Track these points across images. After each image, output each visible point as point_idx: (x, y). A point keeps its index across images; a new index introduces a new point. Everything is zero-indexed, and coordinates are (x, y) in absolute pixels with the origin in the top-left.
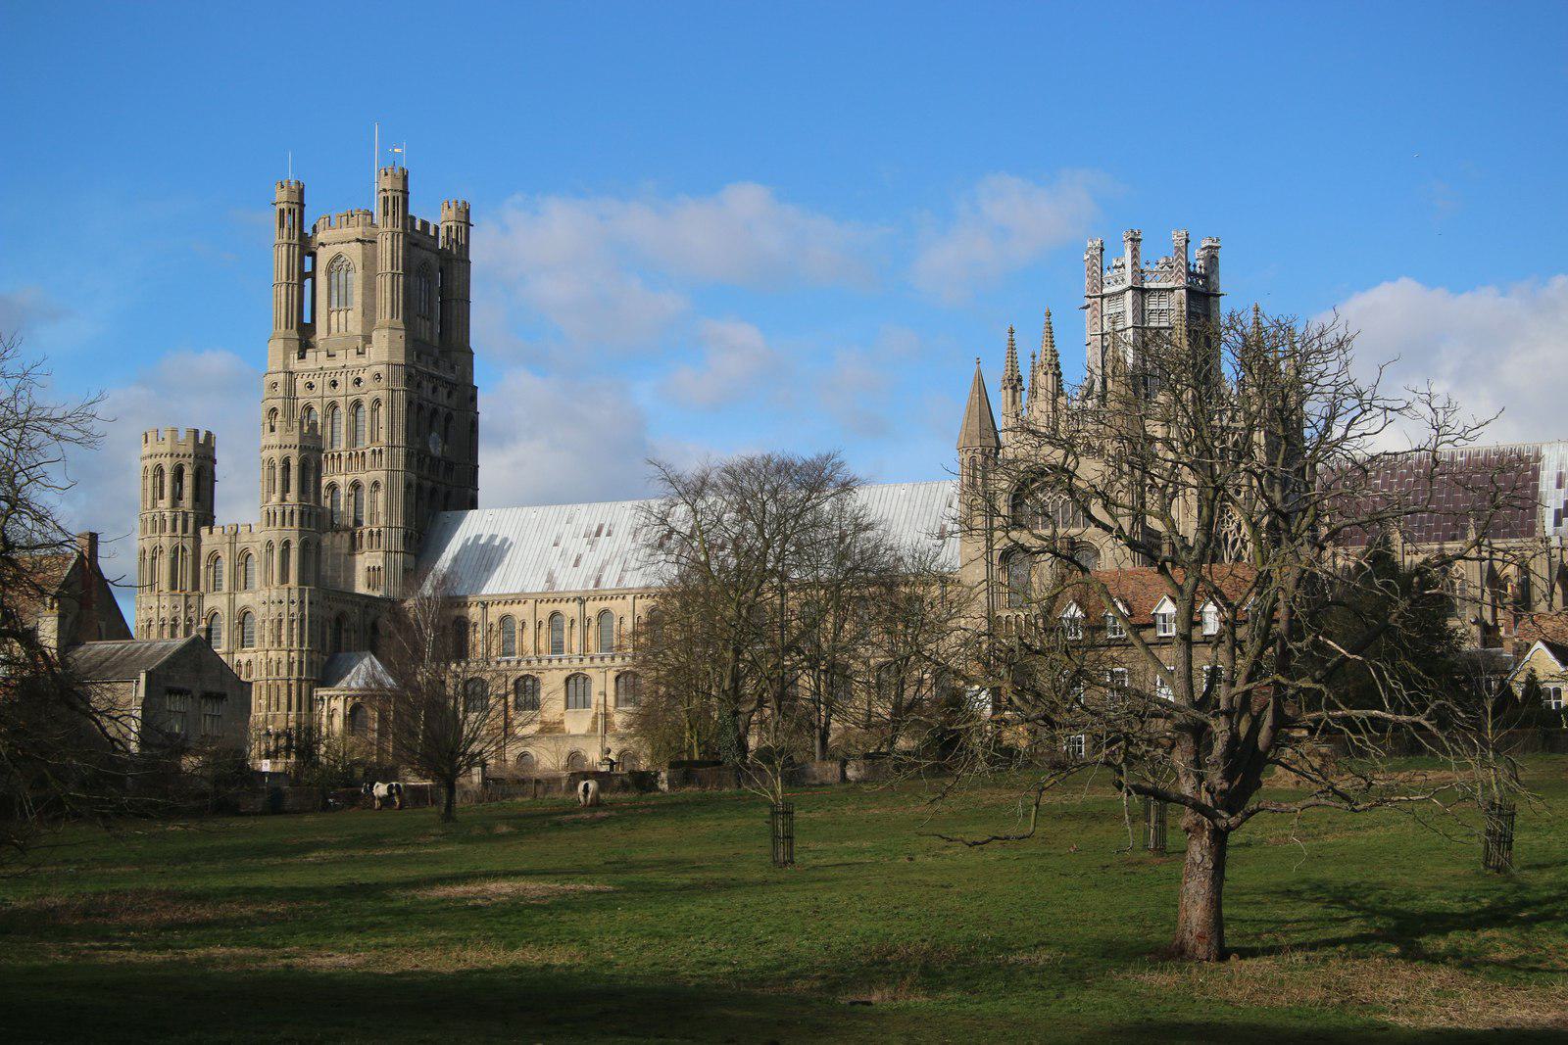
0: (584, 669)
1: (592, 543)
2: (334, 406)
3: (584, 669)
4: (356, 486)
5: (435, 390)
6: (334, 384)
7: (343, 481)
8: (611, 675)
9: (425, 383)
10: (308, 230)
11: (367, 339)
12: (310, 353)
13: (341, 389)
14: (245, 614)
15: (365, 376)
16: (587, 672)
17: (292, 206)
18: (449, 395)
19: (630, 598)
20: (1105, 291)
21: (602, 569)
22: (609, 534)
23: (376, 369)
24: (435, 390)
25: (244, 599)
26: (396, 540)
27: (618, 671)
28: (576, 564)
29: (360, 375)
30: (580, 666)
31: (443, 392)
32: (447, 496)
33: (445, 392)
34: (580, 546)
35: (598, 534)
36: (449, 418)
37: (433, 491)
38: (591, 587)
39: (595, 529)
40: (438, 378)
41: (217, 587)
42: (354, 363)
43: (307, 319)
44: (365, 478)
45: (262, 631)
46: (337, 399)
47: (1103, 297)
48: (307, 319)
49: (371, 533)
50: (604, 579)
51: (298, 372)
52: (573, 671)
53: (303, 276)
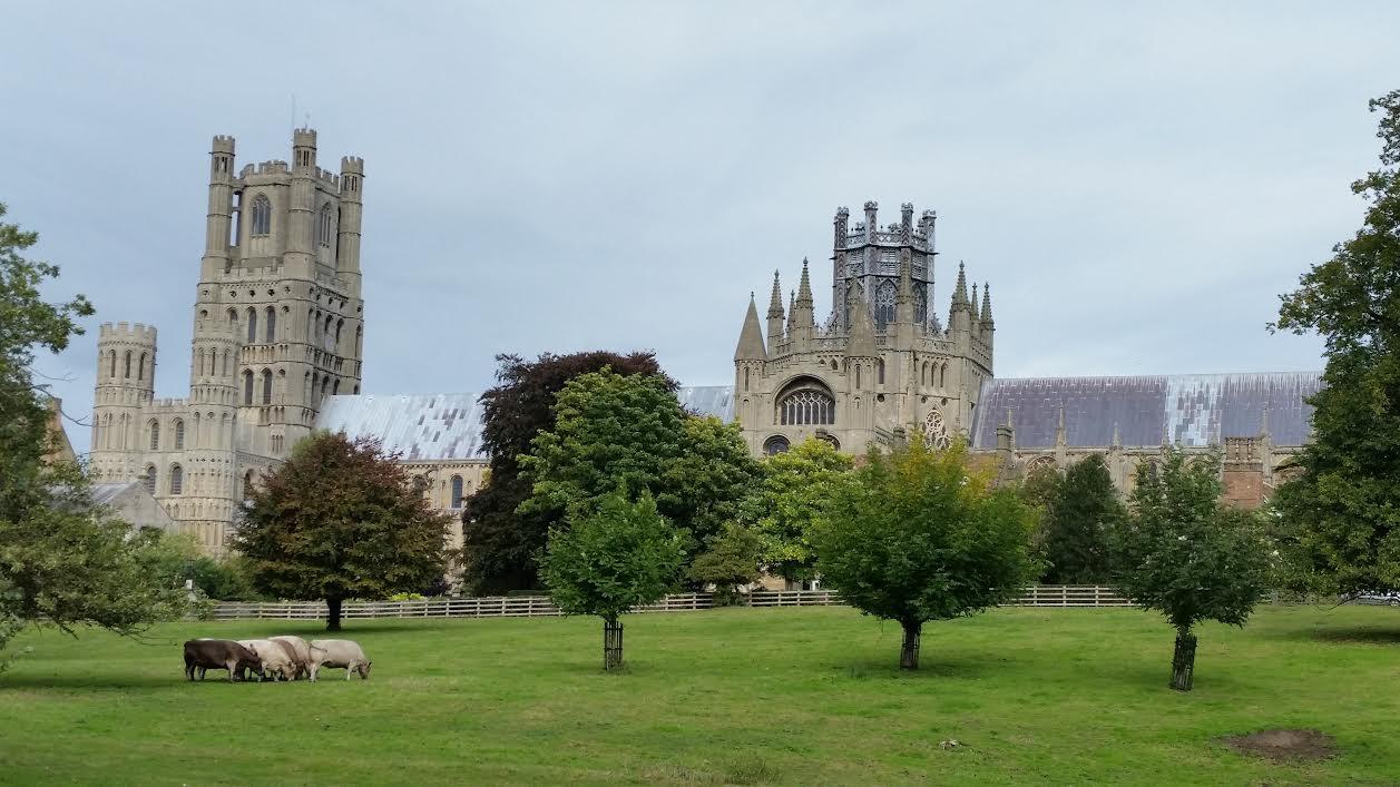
1: (449, 424)
2: (252, 311)
4: (267, 373)
5: (331, 301)
6: (253, 293)
7: (257, 369)
9: (323, 296)
10: (237, 174)
11: (280, 261)
12: (234, 271)
13: (256, 298)
14: (177, 468)
15: (276, 289)
17: (225, 156)
18: (342, 305)
20: (849, 247)
21: (455, 444)
24: (331, 301)
25: (176, 457)
26: (293, 414)
28: (435, 440)
31: (336, 303)
32: (337, 382)
33: (339, 303)
34: (440, 425)
35: (454, 416)
36: (340, 323)
37: (326, 380)
38: (447, 454)
39: (451, 412)
41: (155, 446)
43: (233, 243)
44: (274, 368)
45: (188, 484)
46: (254, 306)
47: (847, 251)
48: (233, 243)
49: (277, 409)
50: (456, 451)
53: (232, 209)
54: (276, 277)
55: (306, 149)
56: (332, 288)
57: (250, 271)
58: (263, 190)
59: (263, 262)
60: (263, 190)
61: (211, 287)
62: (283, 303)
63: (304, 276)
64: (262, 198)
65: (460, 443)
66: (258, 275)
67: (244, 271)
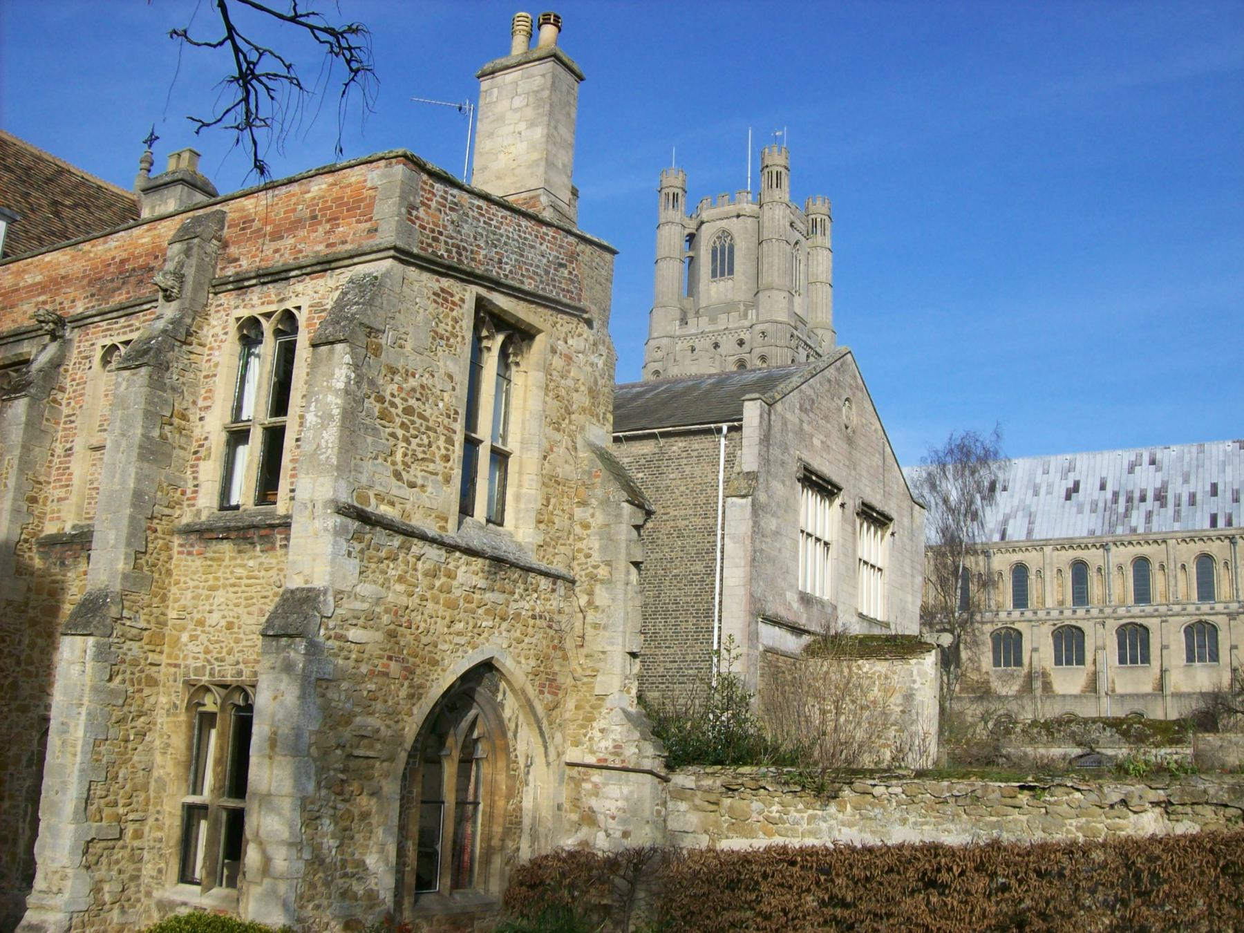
0: (1013, 623)
3: (1013, 623)
6: (716, 346)
8: (1047, 629)
12: (692, 321)
16: (1016, 626)
17: (676, 191)
19: (1048, 550)
22: (1005, 489)
23: (759, 328)
27: (1055, 625)
29: (742, 336)
30: (1008, 619)
40: (810, 347)
42: (736, 325)
50: (1009, 532)
51: (679, 337)
52: (1000, 625)
54: (747, 323)
55: (779, 169)
56: (809, 342)
57: (713, 320)
58: (724, 224)
59: (729, 307)
60: (724, 224)
61: (665, 341)
62: (758, 351)
63: (783, 317)
64: (725, 234)
65: (1011, 522)
66: (723, 321)
67: (704, 321)
